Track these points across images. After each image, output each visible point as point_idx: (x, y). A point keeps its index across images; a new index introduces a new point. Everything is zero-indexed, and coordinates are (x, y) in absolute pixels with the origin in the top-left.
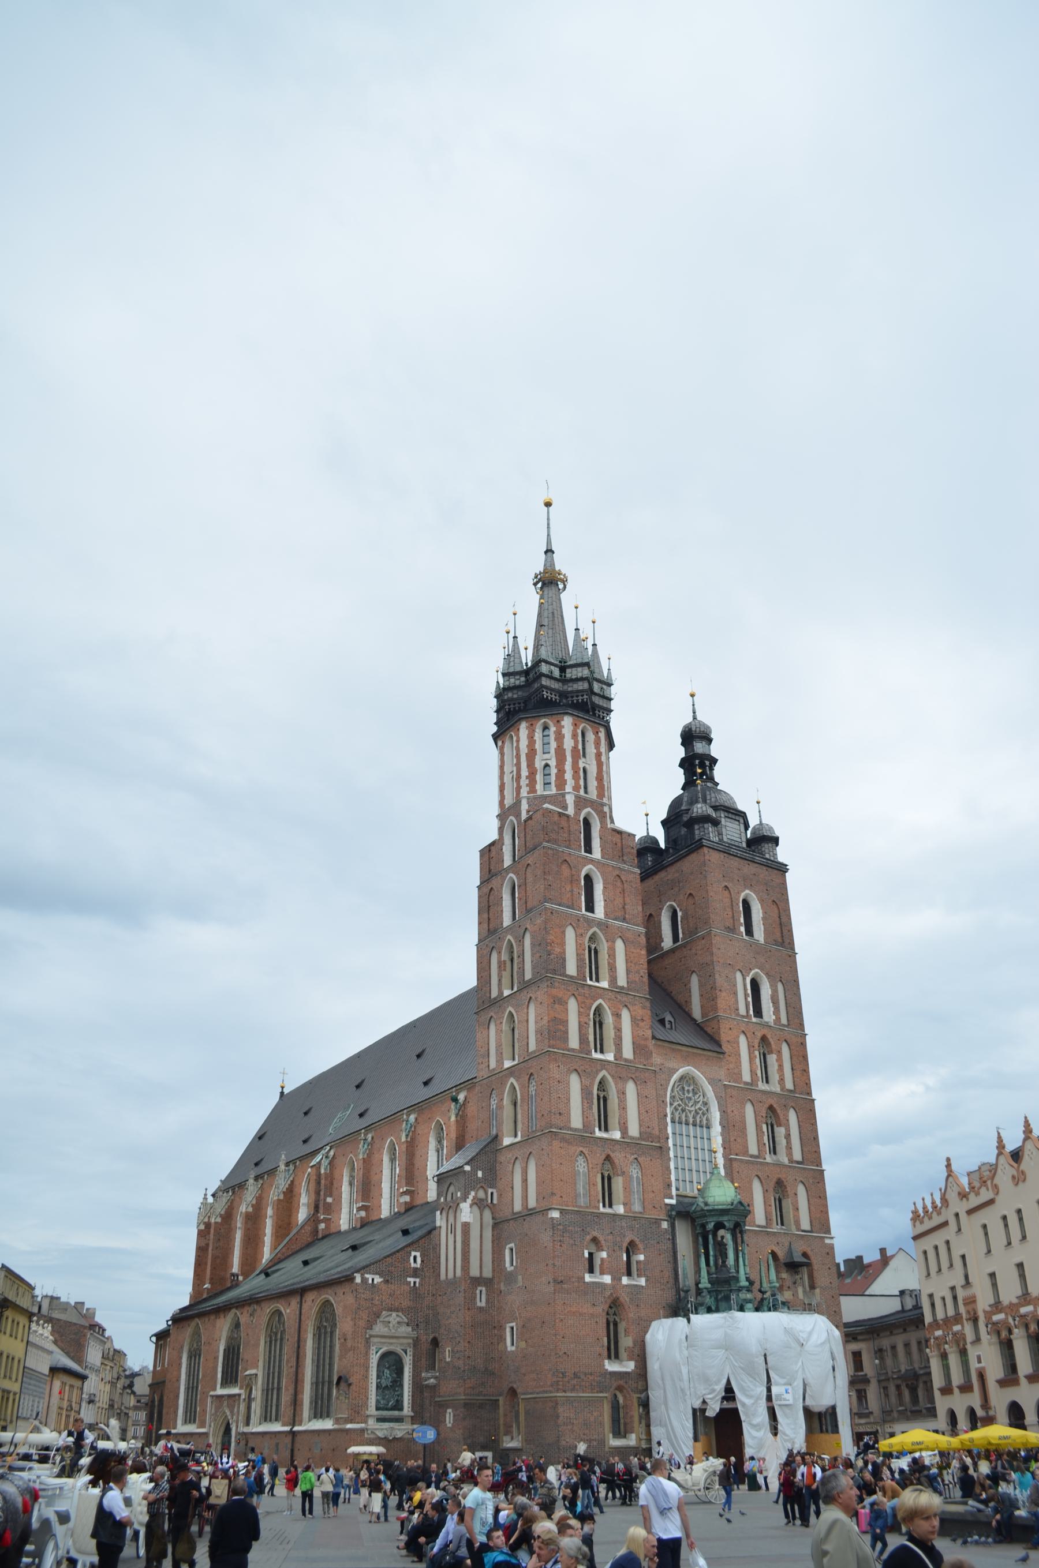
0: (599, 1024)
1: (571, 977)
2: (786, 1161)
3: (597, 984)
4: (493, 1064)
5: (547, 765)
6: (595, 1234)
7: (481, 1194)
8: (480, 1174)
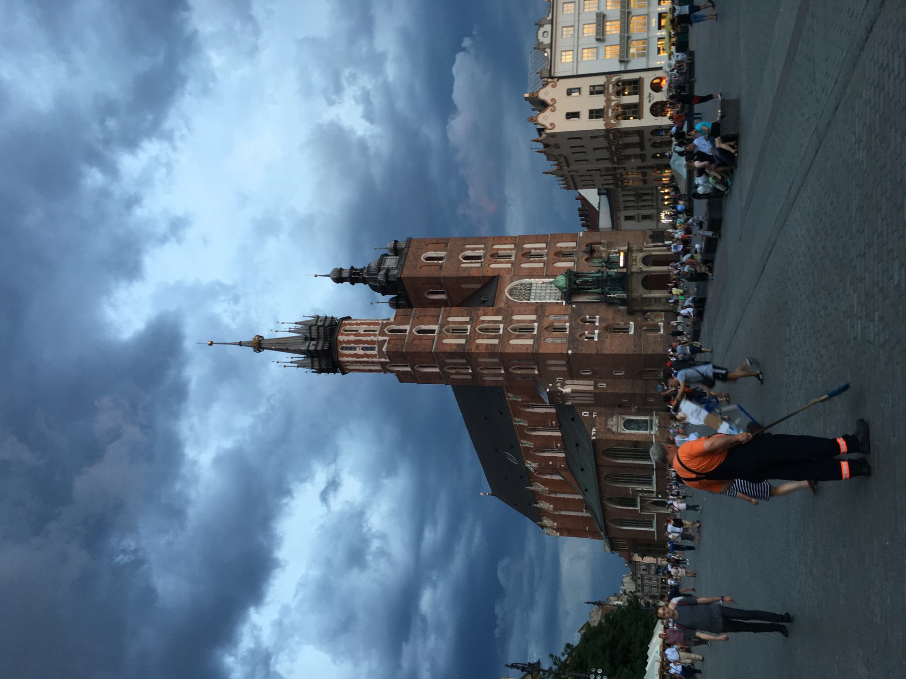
0: (486, 330)
1: (466, 342)
2: (546, 251)
3: (469, 330)
4: (501, 379)
5: (362, 349)
6: (578, 336)
7: (559, 385)
8: (550, 385)
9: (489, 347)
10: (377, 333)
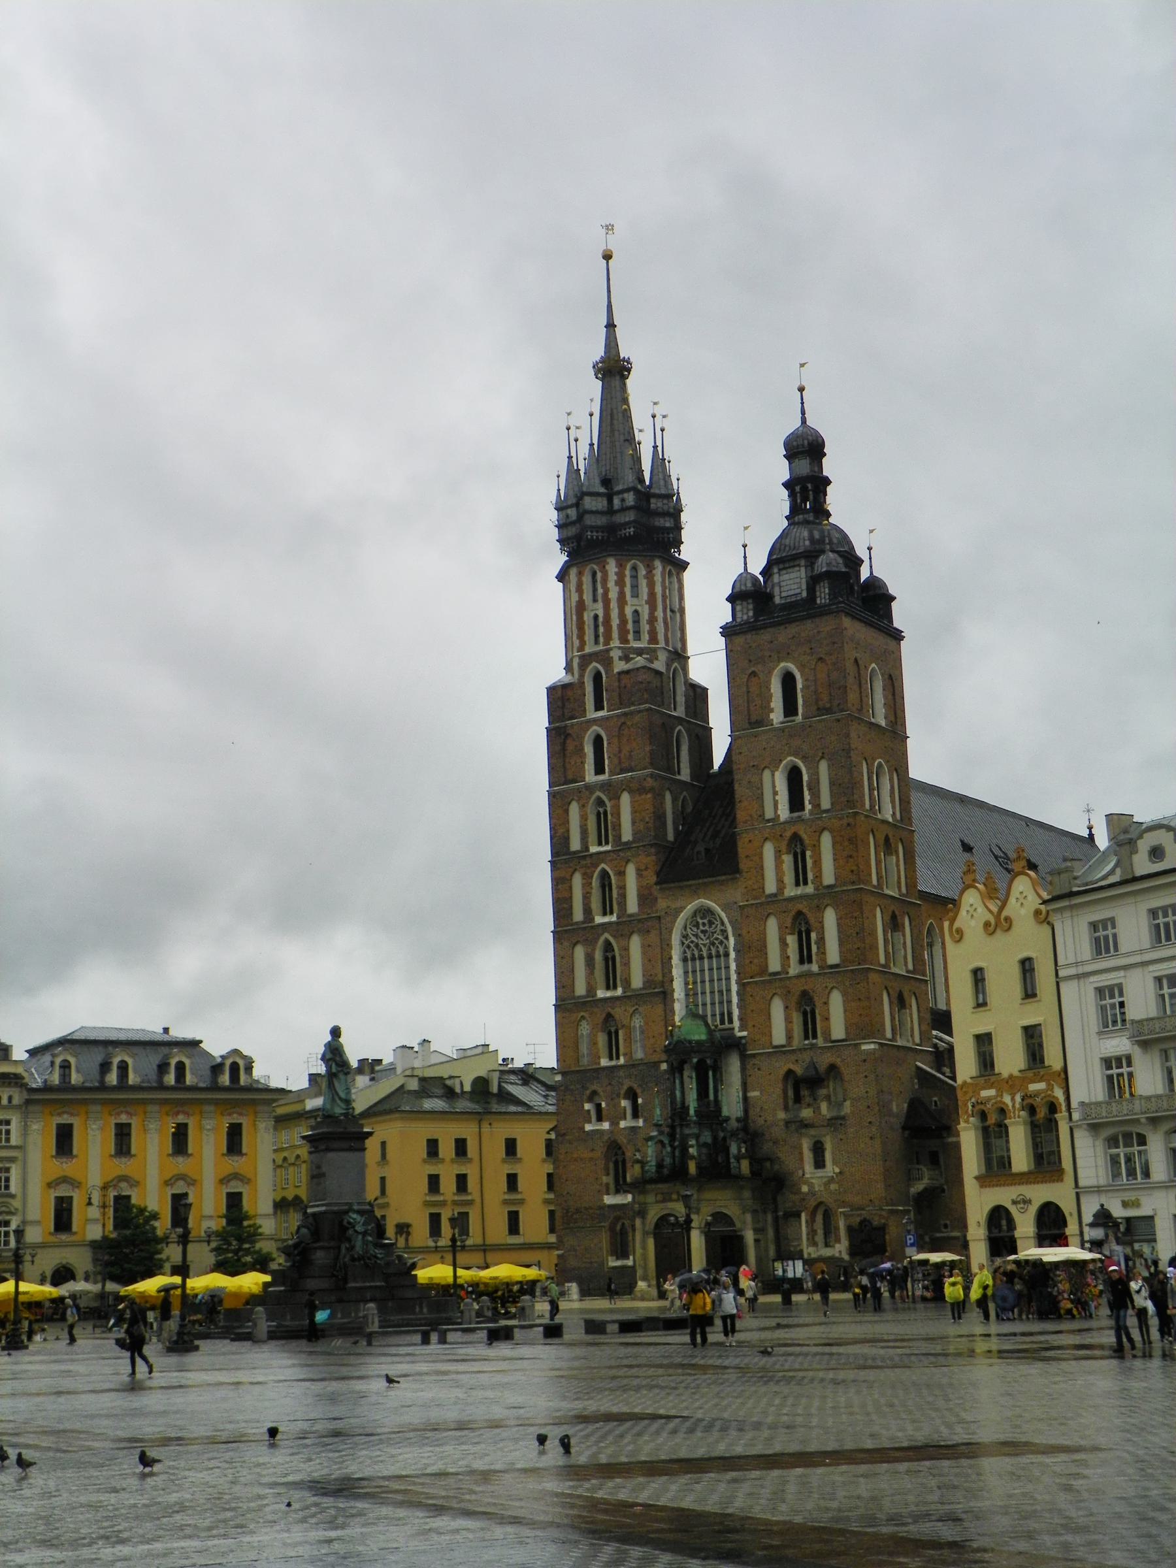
1: (575, 853)
2: (815, 968)
6: (594, 1087)
9: (565, 906)
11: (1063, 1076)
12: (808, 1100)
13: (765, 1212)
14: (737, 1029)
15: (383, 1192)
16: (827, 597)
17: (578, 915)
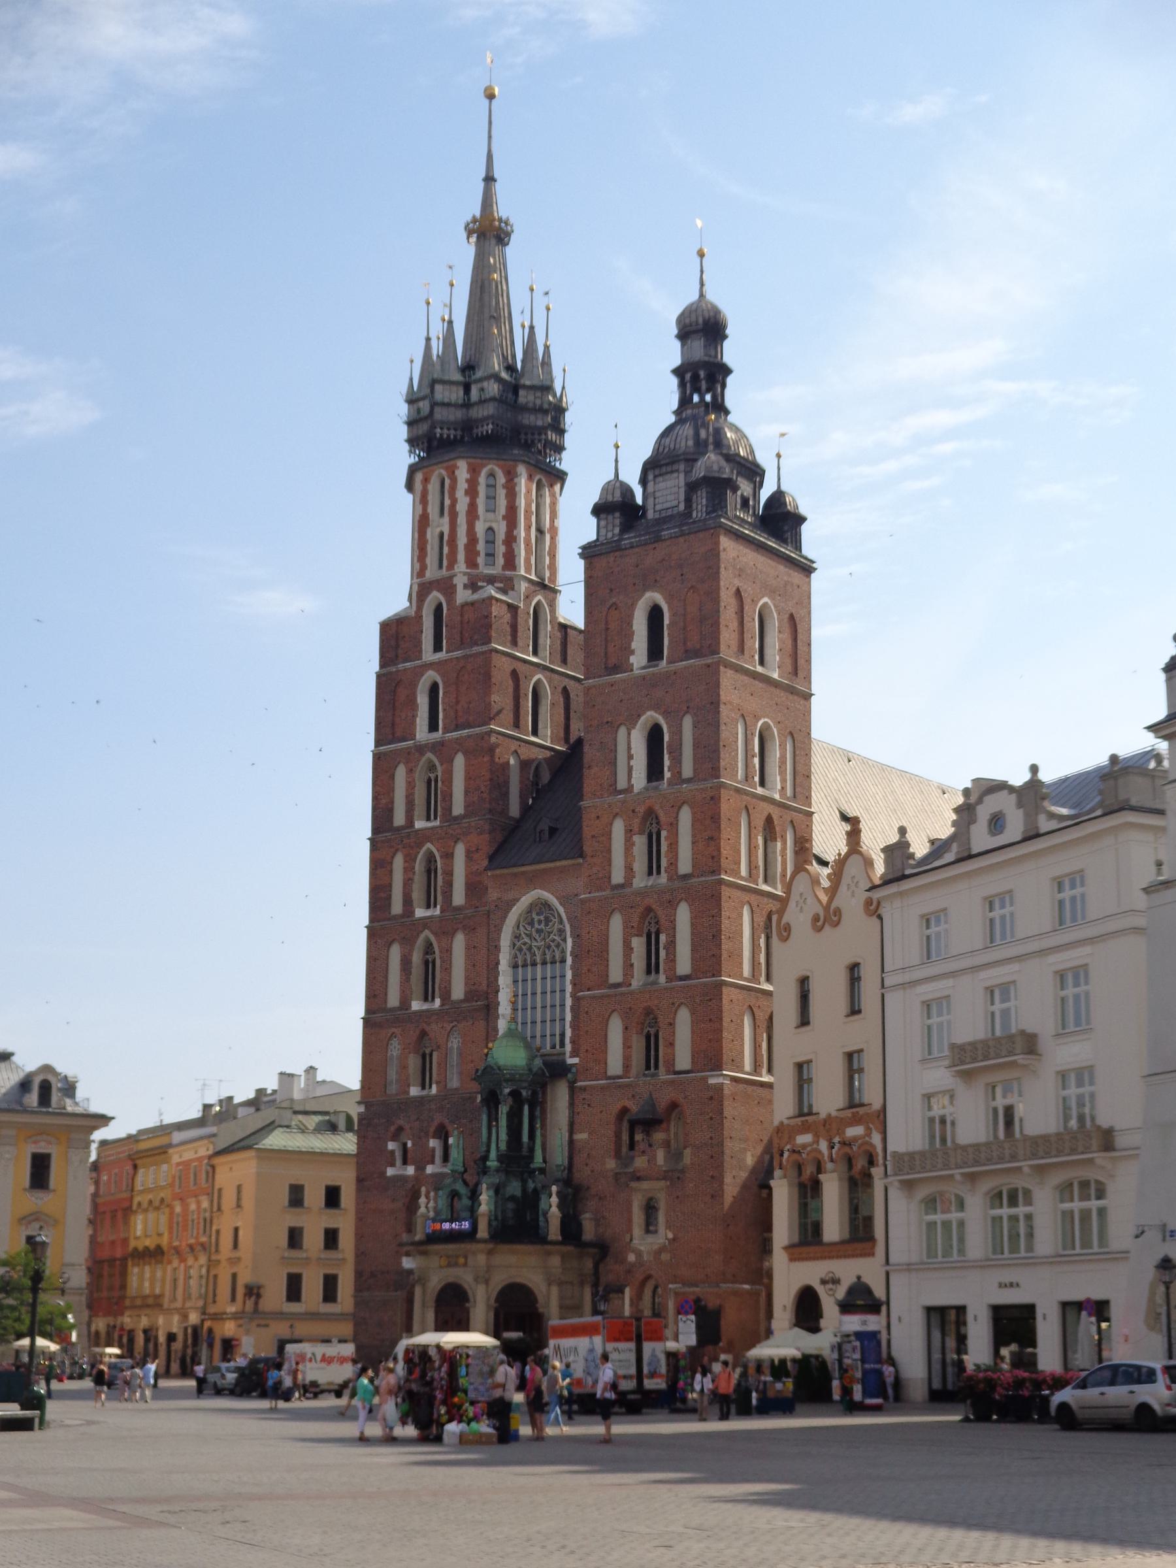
2: (662, 978)
6: (401, 1122)
9: (382, 895)
10: (431, 573)
11: (882, 1117)
12: (642, 1146)
13: (582, 1284)
14: (568, 1054)
15: (236, 1245)
16: (704, 509)
17: (397, 908)
